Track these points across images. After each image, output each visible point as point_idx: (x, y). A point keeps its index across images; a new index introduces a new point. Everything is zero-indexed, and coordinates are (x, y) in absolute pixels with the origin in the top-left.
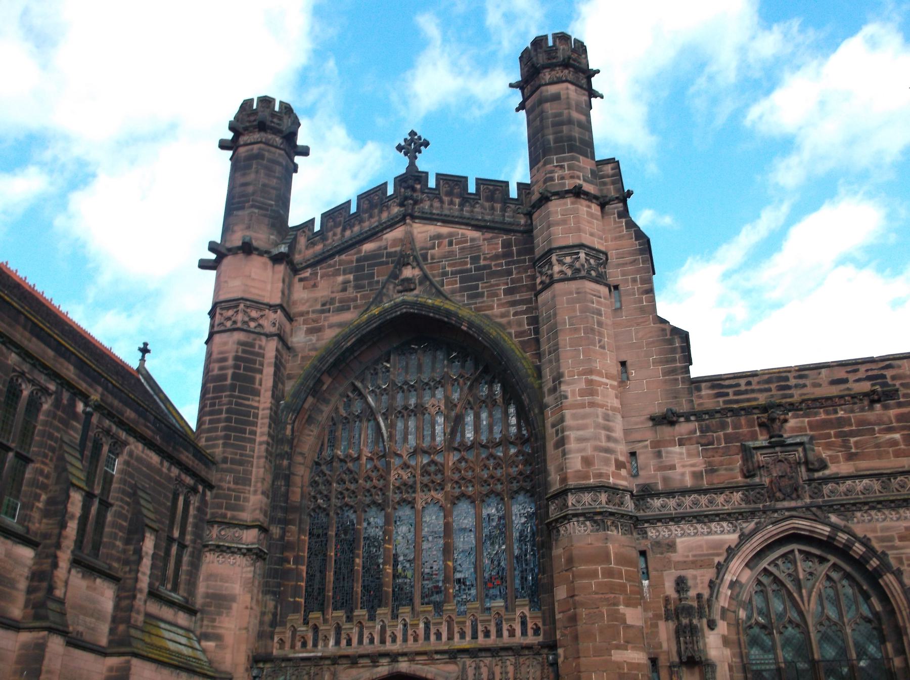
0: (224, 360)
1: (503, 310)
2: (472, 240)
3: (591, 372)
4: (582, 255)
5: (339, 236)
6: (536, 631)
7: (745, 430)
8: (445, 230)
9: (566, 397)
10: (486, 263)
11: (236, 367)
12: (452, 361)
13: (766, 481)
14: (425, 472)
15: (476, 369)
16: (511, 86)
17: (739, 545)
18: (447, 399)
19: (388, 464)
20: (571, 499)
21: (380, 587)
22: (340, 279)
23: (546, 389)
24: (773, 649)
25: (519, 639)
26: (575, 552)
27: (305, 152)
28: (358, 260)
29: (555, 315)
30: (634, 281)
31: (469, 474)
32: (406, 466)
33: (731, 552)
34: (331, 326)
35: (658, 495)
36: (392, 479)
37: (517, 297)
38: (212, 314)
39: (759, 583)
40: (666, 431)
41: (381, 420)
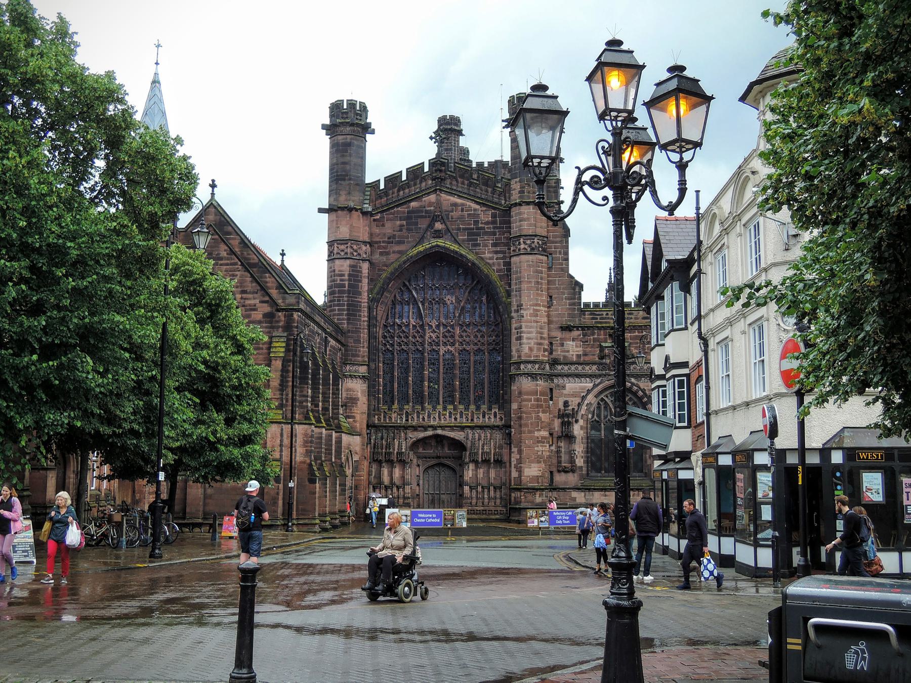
0: (343, 275)
1: (491, 255)
2: (475, 210)
3: (537, 305)
4: (536, 241)
5: (396, 194)
6: (501, 419)
7: (602, 337)
8: (459, 201)
9: (523, 317)
10: (483, 226)
11: (349, 280)
12: (459, 275)
13: (608, 361)
14: (445, 337)
15: (473, 281)
16: (503, 121)
17: (592, 389)
18: (457, 298)
19: (424, 330)
20: (522, 366)
21: (423, 391)
22: (398, 223)
23: (513, 309)
24: (600, 431)
25: (493, 421)
26: (523, 390)
27: (373, 132)
28: (408, 212)
29: (520, 272)
30: (560, 253)
31: (468, 339)
32: (434, 332)
33: (589, 391)
34: (394, 252)
35: (560, 364)
36: (427, 338)
37: (498, 249)
38: (331, 244)
39: (599, 404)
40: (566, 334)
41: (420, 305)
